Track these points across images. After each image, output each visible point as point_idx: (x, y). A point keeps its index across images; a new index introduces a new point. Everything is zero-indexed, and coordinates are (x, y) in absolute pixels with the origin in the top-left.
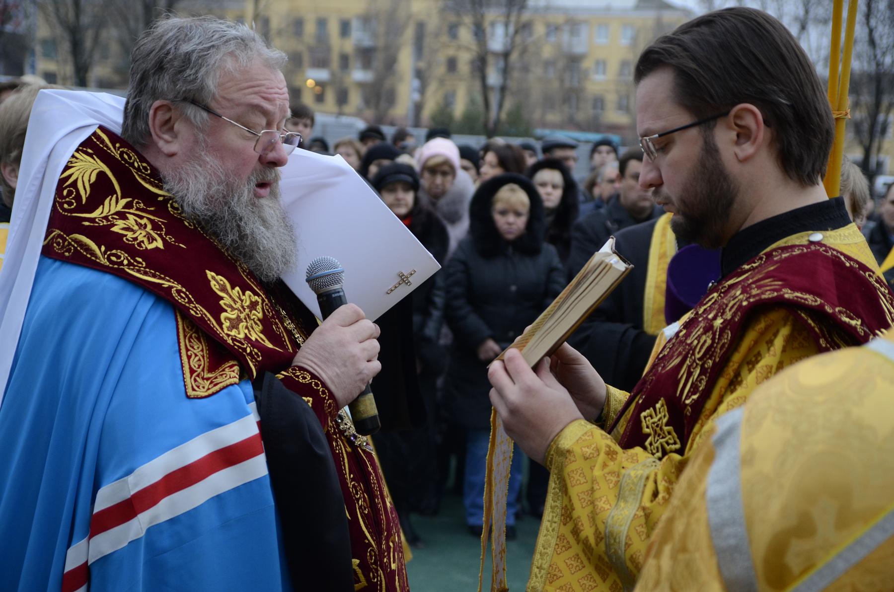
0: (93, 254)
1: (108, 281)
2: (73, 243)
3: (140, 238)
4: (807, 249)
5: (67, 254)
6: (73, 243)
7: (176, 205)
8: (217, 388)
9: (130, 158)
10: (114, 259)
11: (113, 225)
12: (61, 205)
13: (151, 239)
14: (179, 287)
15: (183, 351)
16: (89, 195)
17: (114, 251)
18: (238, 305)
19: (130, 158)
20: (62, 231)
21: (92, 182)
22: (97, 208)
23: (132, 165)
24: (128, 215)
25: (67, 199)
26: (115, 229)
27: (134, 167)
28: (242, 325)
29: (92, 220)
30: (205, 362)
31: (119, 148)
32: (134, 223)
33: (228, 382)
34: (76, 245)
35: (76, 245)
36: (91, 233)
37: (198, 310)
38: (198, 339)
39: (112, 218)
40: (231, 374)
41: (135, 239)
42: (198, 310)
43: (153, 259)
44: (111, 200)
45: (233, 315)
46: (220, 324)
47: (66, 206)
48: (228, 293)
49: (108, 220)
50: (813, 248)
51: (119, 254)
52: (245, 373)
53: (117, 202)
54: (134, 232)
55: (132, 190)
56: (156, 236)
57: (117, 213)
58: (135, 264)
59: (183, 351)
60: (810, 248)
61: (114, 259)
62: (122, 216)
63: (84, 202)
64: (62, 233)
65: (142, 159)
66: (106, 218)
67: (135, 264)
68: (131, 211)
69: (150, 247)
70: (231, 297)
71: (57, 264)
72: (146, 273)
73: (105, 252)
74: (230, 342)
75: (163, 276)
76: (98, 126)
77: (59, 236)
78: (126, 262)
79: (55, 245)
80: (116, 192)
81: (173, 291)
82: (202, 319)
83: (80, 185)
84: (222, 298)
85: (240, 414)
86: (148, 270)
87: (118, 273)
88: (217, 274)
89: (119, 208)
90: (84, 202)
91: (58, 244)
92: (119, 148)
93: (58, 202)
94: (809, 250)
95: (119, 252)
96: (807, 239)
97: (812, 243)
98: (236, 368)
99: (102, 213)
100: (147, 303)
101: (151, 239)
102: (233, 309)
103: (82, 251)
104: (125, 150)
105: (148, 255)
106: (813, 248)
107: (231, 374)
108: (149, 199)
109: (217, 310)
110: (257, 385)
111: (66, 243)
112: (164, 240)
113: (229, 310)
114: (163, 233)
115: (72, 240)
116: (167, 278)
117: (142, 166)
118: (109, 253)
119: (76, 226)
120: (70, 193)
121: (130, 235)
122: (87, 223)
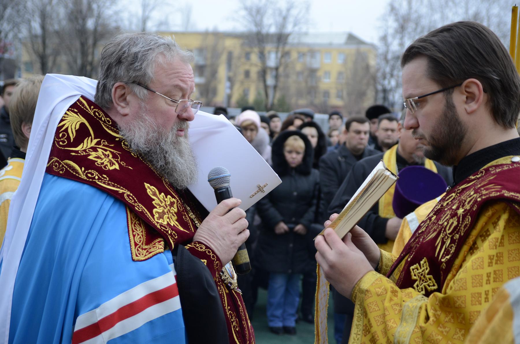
0: (77, 172)
1: (86, 189)
2: (65, 166)
3: (105, 163)
4: (512, 166)
5: (61, 172)
6: (65, 166)
7: (126, 143)
8: (151, 255)
9: (99, 115)
10: (89, 175)
11: (89, 155)
12: (58, 142)
13: (112, 164)
14: (129, 193)
15: (131, 232)
16: (75, 137)
17: (90, 171)
18: (163, 204)
19: (99, 115)
20: (58, 158)
21: (76, 129)
22: (80, 144)
23: (101, 119)
24: (98, 149)
25: (62, 139)
26: (90, 157)
27: (102, 120)
28: (166, 216)
29: (77, 152)
30: (144, 239)
31: (93, 109)
32: (101, 153)
33: (158, 251)
34: (67, 167)
35: (67, 167)
36: (75, 159)
37: (140, 207)
38: (140, 225)
39: (89, 151)
40: (159, 246)
41: (102, 163)
42: (140, 207)
44: (88, 140)
45: (160, 210)
46: (153, 216)
47: (61, 143)
48: (157, 197)
49: (86, 152)
50: (515, 165)
51: (93, 172)
52: (167, 246)
53: (91, 141)
54: (101, 158)
55: (100, 134)
57: (91, 148)
58: (102, 178)
59: (131, 232)
60: (514, 166)
61: (89, 175)
62: (94, 149)
64: (58, 160)
65: (107, 116)
66: (85, 151)
67: (102, 178)
68: (100, 146)
69: (112, 168)
70: (159, 199)
71: (55, 178)
72: (109, 184)
73: (84, 171)
74: (159, 227)
75: (119, 186)
76: (81, 96)
77: (57, 161)
78: (97, 177)
79: (54, 166)
80: (91, 135)
81: (125, 195)
82: (142, 213)
83: (69, 131)
84: (154, 200)
85: (165, 271)
86: (110, 182)
87: (92, 184)
88: (151, 185)
89: (93, 144)
91: (56, 166)
92: (93, 109)
93: (57, 141)
94: (513, 167)
95: (93, 171)
96: (510, 160)
97: (513, 163)
98: (162, 243)
99: (83, 147)
100: (110, 202)
101: (112, 164)
102: (160, 206)
103: (70, 170)
104: (97, 110)
105: (110, 174)
106: (515, 165)
107: (159, 246)
109: (151, 207)
111: (61, 166)
112: (119, 164)
113: (158, 207)
114: (119, 160)
115: (65, 164)
116: (122, 187)
117: (107, 120)
118: (86, 172)
120: (63, 136)
122: (73, 154)
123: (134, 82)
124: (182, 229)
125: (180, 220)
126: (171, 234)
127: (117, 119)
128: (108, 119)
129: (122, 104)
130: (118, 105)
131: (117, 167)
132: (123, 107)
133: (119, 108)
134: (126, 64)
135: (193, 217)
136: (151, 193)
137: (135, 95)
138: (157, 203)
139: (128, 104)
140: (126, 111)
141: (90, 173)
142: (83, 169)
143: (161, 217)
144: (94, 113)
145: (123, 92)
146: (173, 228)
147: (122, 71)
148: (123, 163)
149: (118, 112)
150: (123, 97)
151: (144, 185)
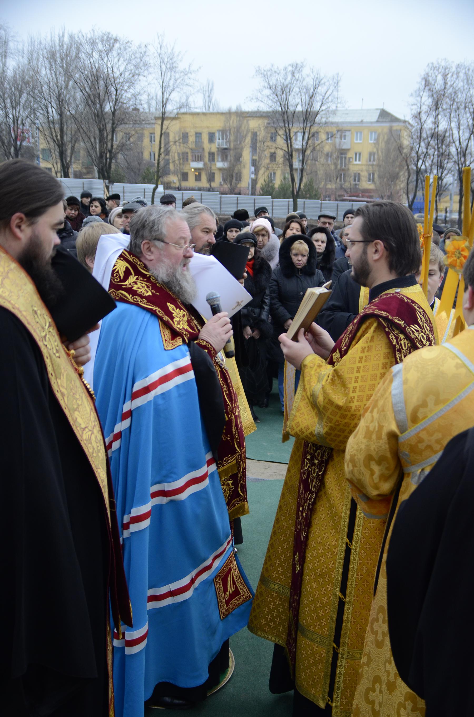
0: (127, 298)
1: (133, 308)
3: (143, 292)
5: (117, 298)
7: (154, 278)
8: (175, 346)
11: (133, 287)
13: (147, 292)
14: (159, 309)
15: (162, 333)
23: (137, 263)
26: (134, 288)
28: (181, 323)
29: (126, 285)
30: (170, 337)
33: (179, 344)
36: (125, 290)
37: (166, 318)
38: (167, 328)
40: (179, 341)
41: (142, 292)
42: (166, 318)
43: (149, 299)
45: (178, 319)
46: (174, 323)
47: (116, 280)
52: (184, 341)
55: (138, 273)
56: (148, 290)
57: (134, 282)
59: (162, 333)
61: (135, 299)
62: (136, 283)
65: (141, 261)
66: (130, 284)
68: (139, 281)
69: (147, 295)
72: (147, 305)
73: (132, 297)
74: (178, 330)
77: (113, 291)
78: (139, 301)
81: (157, 311)
82: (168, 321)
83: (120, 272)
84: (173, 313)
85: (184, 356)
87: (138, 305)
89: (134, 280)
91: (113, 294)
95: (137, 297)
98: (181, 339)
100: (148, 316)
101: (147, 292)
102: (178, 317)
105: (147, 298)
107: (179, 341)
108: (144, 276)
109: (172, 318)
110: (189, 345)
112: (152, 293)
114: (151, 289)
119: (119, 287)
120: (117, 275)
121: (139, 290)
123: (155, 239)
124: (191, 331)
125: (189, 325)
126: (185, 334)
127: (147, 263)
129: (149, 253)
130: (147, 254)
132: (149, 255)
133: (147, 257)
134: (149, 228)
135: (196, 323)
137: (156, 247)
139: (152, 253)
140: (152, 257)
141: (135, 298)
143: (178, 323)
144: (133, 259)
145: (148, 246)
146: (186, 330)
147: (146, 233)
148: (153, 291)
149: (146, 259)
150: (149, 249)
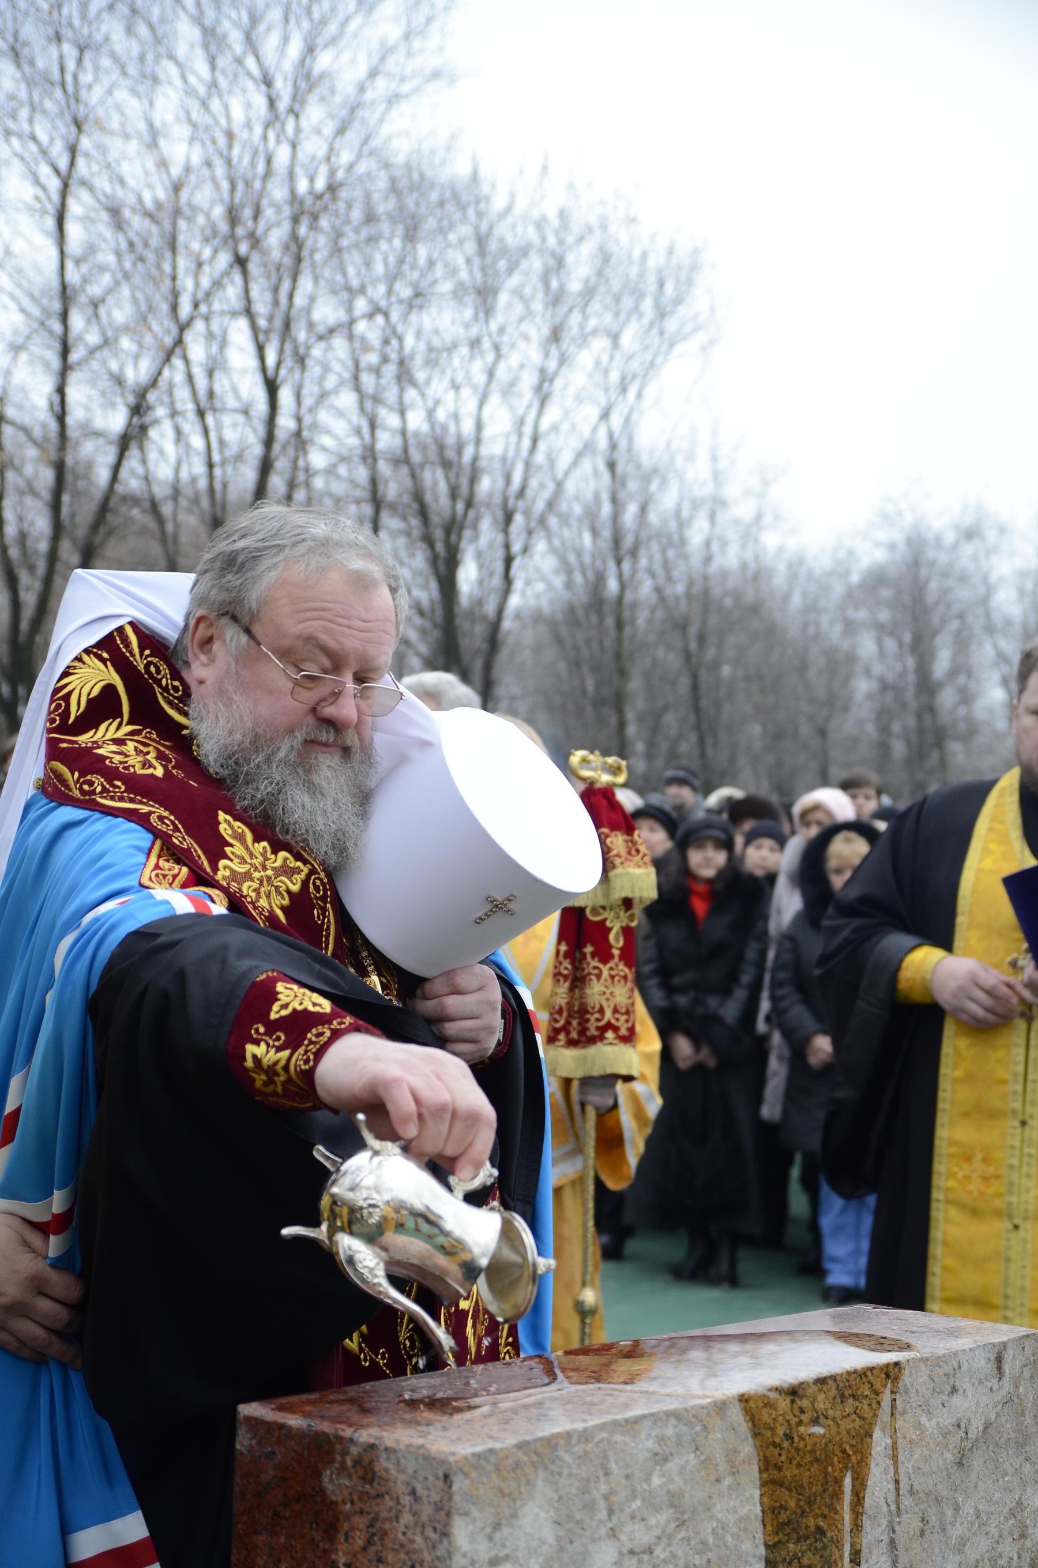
16: (82, 713)
19: (158, 672)
21: (91, 696)
22: (86, 731)
27: (160, 685)
31: (147, 656)
63: (70, 722)
90: (70, 722)
104: (155, 660)
122: (65, 745)
128: (176, 683)
131: (159, 772)
136: (230, 832)
138: (238, 853)
142: (76, 774)
144: (147, 666)
151: (217, 815)
